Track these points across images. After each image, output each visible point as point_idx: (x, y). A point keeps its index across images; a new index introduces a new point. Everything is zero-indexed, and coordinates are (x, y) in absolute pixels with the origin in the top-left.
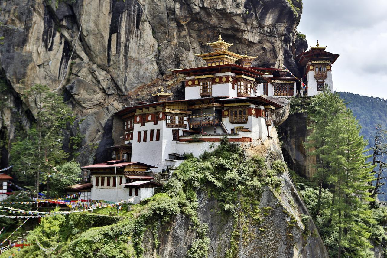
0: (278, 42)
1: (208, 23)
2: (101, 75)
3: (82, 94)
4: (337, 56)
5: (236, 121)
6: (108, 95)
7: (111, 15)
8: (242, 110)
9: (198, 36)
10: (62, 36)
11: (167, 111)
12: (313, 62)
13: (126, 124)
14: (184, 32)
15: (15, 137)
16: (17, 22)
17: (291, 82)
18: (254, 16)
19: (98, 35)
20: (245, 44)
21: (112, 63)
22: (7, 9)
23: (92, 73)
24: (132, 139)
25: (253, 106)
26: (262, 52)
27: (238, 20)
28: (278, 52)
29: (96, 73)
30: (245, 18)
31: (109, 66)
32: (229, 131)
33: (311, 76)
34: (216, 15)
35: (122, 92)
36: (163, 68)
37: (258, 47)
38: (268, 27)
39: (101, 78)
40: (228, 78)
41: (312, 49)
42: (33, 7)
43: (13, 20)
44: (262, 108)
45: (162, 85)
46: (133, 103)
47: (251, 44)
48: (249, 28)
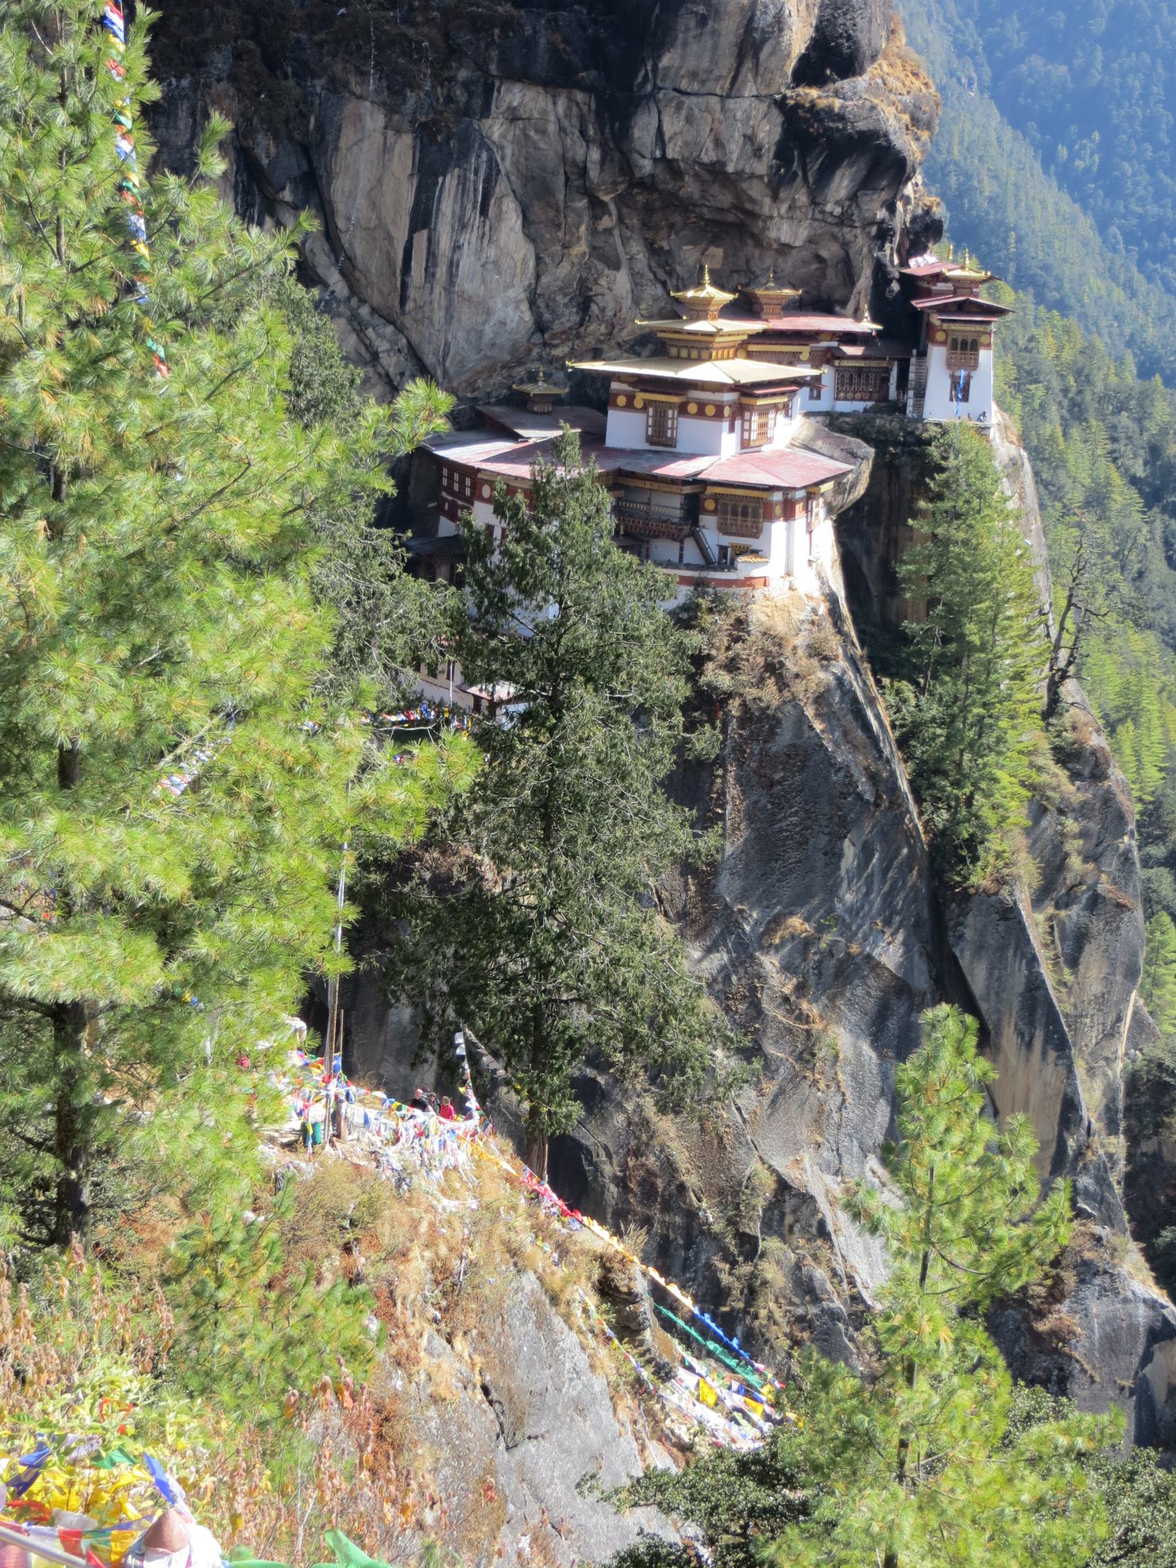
1: (674, 195)
7: (415, 182)
9: (645, 225)
13: (445, 472)
14: (606, 219)
17: (884, 364)
18: (799, 179)
19: (379, 232)
21: (410, 305)
25: (777, 497)
26: (814, 266)
27: (756, 190)
29: (370, 332)
30: (777, 185)
31: (403, 313)
32: (714, 553)
33: (937, 354)
34: (697, 176)
36: (547, 316)
38: (837, 203)
39: (382, 346)
40: (719, 408)
45: (540, 358)
47: (785, 249)
48: (784, 208)
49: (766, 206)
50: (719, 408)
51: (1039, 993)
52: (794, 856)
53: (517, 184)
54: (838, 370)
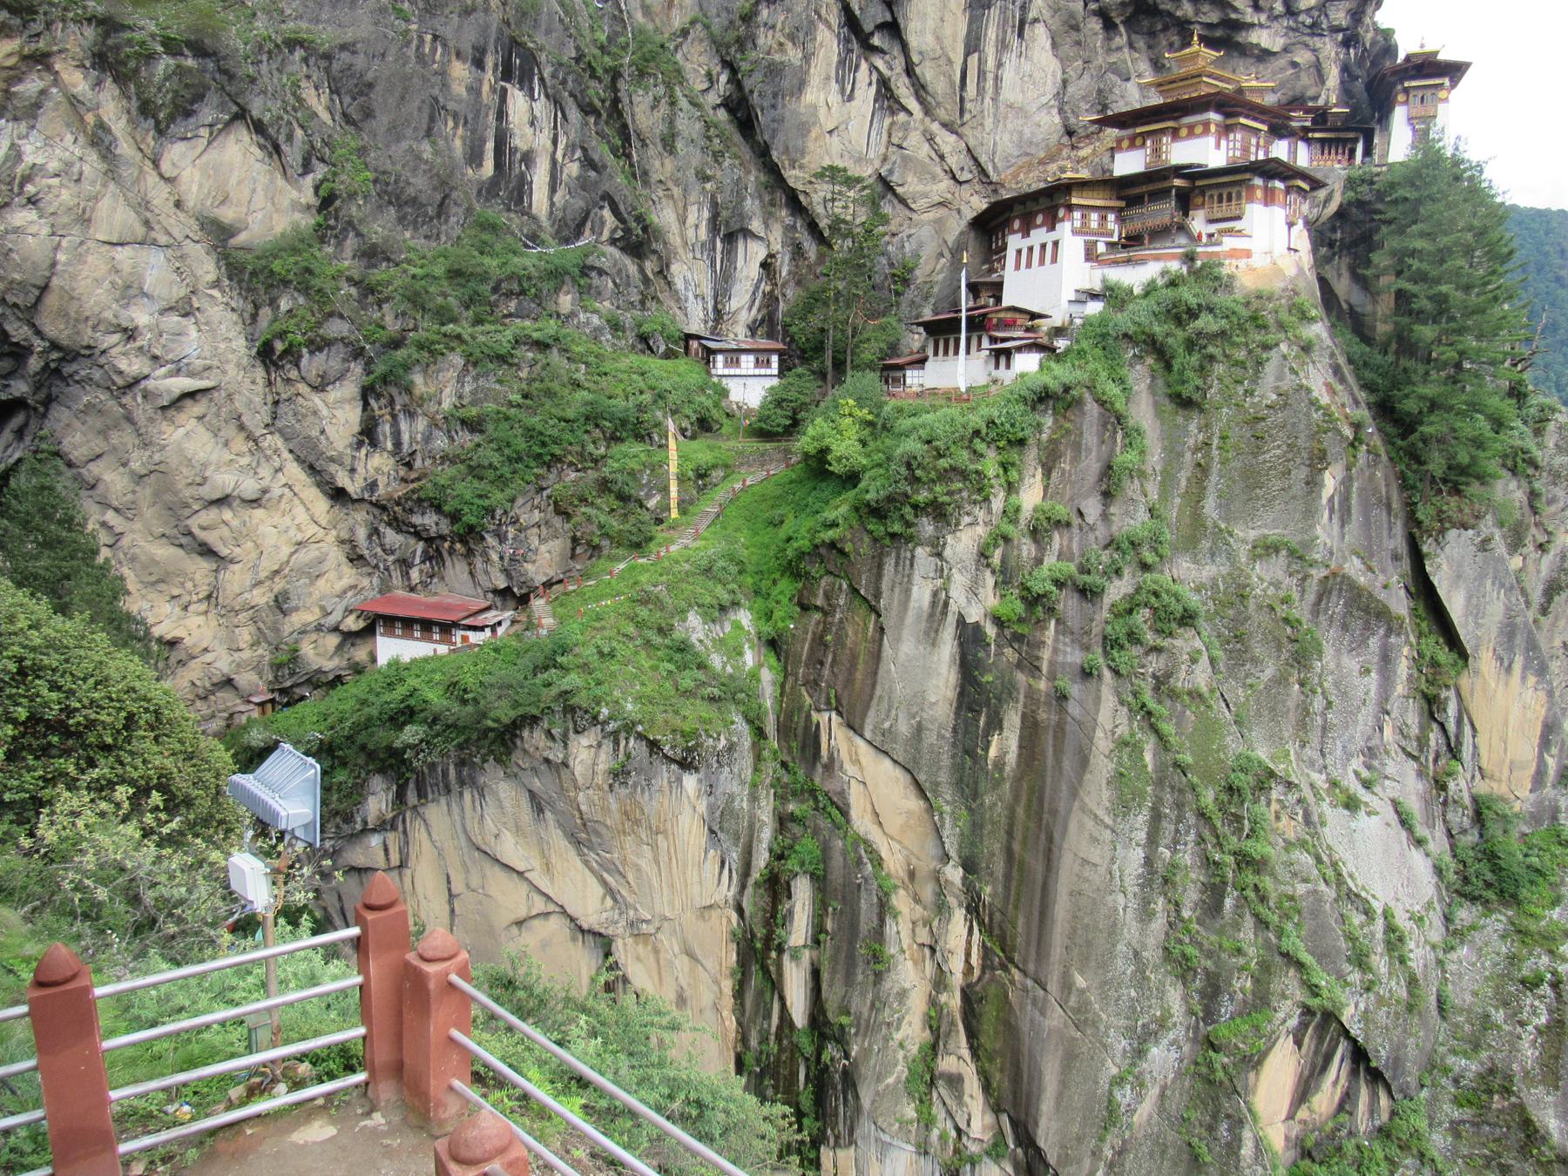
0: (1328, 46)
1: (1170, 14)
2: (947, 141)
3: (910, 185)
4: (1468, 65)
5: (1219, 215)
6: (960, 183)
8: (1234, 191)
9: (1150, 47)
10: (873, 68)
11: (1074, 201)
12: (1406, 84)
14: (1117, 39)
15: (790, 273)
16: (790, 45)
17: (1351, 135)
20: (1252, 55)
21: (967, 116)
22: (770, 22)
23: (931, 140)
24: (1003, 268)
25: (1258, 181)
28: (1325, 71)
29: (938, 139)
35: (987, 176)
36: (1072, 120)
37: (1282, 62)
39: (946, 149)
41: (1408, 58)
42: (817, 12)
43: (781, 44)
44: (1279, 185)
46: (1006, 195)
47: (1265, 55)
48: (1263, 18)
49: (1250, 16)
50: (1206, 125)
51: (1519, 620)
52: (1276, 484)
53: (1047, 14)
54: (1308, 141)
